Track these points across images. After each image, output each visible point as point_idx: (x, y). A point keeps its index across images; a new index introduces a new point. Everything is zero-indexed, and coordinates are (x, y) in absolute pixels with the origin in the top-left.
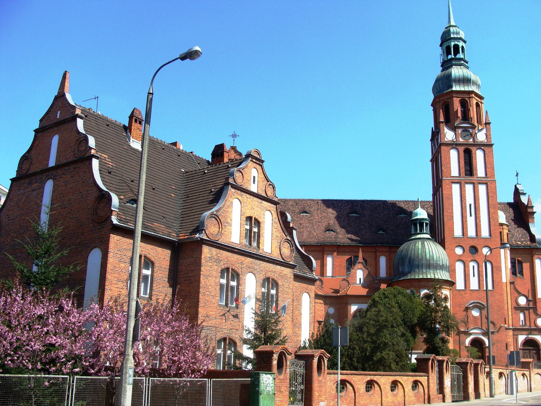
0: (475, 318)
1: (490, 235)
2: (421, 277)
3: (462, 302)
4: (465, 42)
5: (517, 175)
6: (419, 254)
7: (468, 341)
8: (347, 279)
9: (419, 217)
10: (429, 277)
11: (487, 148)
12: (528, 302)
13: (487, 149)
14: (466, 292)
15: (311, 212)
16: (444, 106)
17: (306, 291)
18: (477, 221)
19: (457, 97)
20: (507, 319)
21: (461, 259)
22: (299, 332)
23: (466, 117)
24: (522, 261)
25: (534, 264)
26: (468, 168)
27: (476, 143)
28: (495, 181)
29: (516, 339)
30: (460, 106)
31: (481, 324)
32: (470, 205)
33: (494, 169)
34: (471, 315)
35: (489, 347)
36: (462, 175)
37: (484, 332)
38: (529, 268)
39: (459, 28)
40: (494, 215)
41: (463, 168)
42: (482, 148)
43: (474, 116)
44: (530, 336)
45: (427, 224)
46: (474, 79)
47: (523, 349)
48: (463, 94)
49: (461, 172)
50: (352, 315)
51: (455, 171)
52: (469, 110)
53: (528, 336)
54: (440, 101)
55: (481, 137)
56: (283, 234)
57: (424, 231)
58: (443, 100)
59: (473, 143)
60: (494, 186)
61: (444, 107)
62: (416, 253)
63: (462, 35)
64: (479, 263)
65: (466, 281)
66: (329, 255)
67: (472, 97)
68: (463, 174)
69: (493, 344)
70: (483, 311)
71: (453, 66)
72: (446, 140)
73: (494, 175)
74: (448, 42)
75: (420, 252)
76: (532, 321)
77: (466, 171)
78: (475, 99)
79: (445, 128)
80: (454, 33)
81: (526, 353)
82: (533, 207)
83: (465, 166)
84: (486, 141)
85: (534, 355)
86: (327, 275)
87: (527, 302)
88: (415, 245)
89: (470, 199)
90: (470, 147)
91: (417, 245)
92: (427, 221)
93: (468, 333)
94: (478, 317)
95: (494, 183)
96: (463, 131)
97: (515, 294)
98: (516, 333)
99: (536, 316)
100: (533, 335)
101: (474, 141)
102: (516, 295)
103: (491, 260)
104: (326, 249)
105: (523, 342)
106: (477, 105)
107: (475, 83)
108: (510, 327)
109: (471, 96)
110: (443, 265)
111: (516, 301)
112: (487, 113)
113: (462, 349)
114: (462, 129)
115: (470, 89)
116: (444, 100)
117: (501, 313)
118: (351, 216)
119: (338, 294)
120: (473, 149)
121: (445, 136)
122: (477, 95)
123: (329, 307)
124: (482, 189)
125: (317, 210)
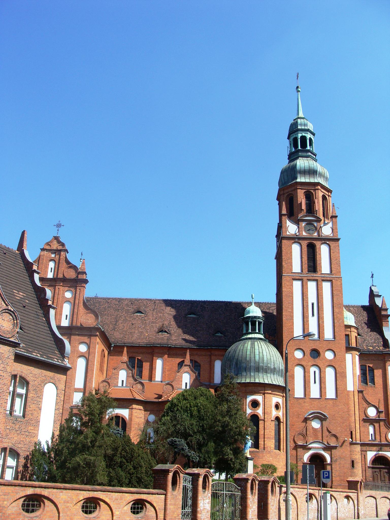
0: (315, 430)
1: (334, 337)
2: (248, 381)
3: (301, 412)
4: (314, 134)
5: (372, 277)
6: (247, 357)
7: (306, 457)
8: (172, 384)
9: (251, 315)
10: (257, 381)
11: (333, 242)
12: (378, 414)
13: (333, 244)
14: (306, 401)
15: (146, 311)
16: (288, 198)
17: (52, 381)
18: (320, 322)
19: (301, 189)
20: (354, 433)
22: (36, 432)
23: (311, 210)
24: (374, 368)
25: (387, 372)
26: (312, 264)
27: (321, 237)
28: (340, 278)
29: (364, 455)
30: (305, 199)
31: (322, 437)
32: (313, 304)
33: (340, 266)
34: (311, 427)
35: (331, 465)
36: (304, 272)
37: (324, 446)
38: (381, 375)
39: (307, 120)
40: (338, 315)
41: (305, 264)
42: (328, 242)
43: (319, 209)
44: (380, 452)
45: (260, 323)
46: (321, 171)
47: (372, 468)
48: (307, 186)
49: (303, 268)
51: (296, 267)
52: (314, 203)
53: (378, 452)
54: (284, 194)
55: (327, 231)
56: (3, 303)
57: (255, 330)
58: (287, 193)
59: (317, 237)
60: (339, 283)
61: (288, 200)
62: (244, 353)
63: (310, 126)
64: (321, 368)
66: (159, 357)
67: (318, 189)
68: (306, 270)
69: (336, 461)
70: (324, 422)
71: (300, 158)
72: (288, 233)
73: (340, 272)
74: (296, 133)
75: (248, 353)
76: (383, 436)
77: (309, 266)
78: (322, 191)
79: (288, 221)
80: (301, 125)
81: (375, 472)
82: (387, 310)
83: (308, 262)
84: (332, 235)
85: (385, 474)
86: (156, 380)
87: (377, 414)
88: (244, 345)
89: (312, 298)
90: (313, 242)
91: (246, 345)
92: (261, 319)
93: (307, 447)
95: (340, 280)
96: (307, 224)
97: (363, 405)
98: (364, 448)
99: (387, 430)
100: (384, 451)
101: (319, 235)
102: (365, 406)
103: (334, 366)
104: (156, 351)
105: (373, 459)
106: (324, 198)
107: (321, 175)
108: (357, 442)
109: (317, 188)
110: (275, 368)
111: (365, 412)
112: (333, 206)
114: (306, 222)
115: (316, 181)
116: (288, 192)
118: (188, 317)
119: (160, 400)
120: (317, 243)
121: (287, 229)
122: (323, 187)
123: (150, 414)
124: (326, 286)
125: (153, 310)
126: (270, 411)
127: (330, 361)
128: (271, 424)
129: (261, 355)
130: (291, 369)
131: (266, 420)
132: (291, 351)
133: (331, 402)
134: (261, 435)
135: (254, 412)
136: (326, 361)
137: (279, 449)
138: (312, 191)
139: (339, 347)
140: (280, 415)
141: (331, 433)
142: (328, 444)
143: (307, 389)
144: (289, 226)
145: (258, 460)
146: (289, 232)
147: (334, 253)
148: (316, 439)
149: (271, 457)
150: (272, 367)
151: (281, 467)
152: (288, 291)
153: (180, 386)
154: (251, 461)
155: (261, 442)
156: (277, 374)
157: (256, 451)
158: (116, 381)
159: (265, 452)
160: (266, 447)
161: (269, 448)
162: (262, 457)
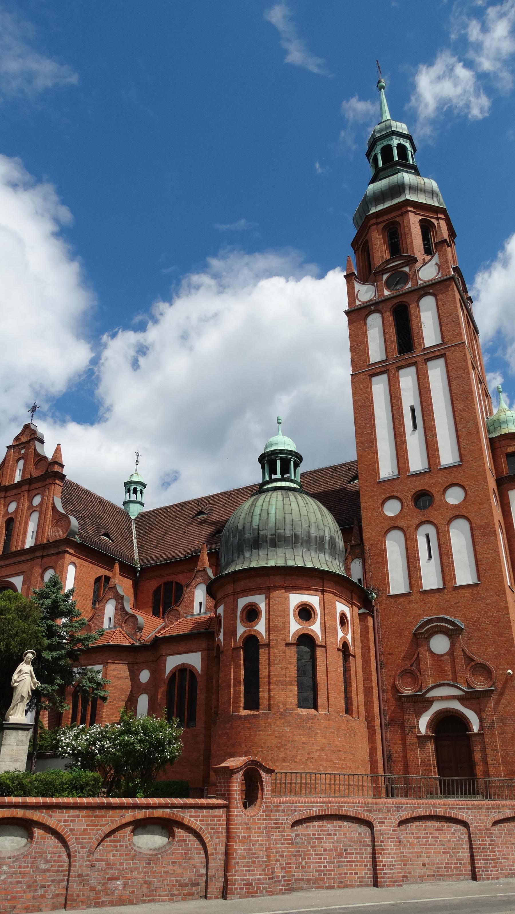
3: (405, 623)
14: (412, 598)
19: (377, 224)
21: (396, 525)
35: (481, 735)
37: (462, 693)
42: (431, 291)
50: (167, 681)
64: (439, 525)
65: (412, 572)
69: (492, 726)
72: (358, 303)
75: (243, 516)
78: (416, 214)
92: (286, 454)
94: (446, 657)
103: (466, 515)
113: (412, 744)
117: (505, 639)
122: (419, 206)
125: (223, 506)
126: (284, 623)
127: (456, 507)
128: (284, 653)
129: (264, 515)
130: (379, 540)
131: (272, 643)
132: (376, 505)
133: (466, 593)
134: (264, 678)
135: (250, 631)
136: (447, 509)
137: (316, 707)
138: (397, 219)
139: (471, 475)
140: (312, 631)
141: (473, 660)
142: (469, 686)
143: (413, 574)
144: (359, 291)
145: (256, 735)
146: (360, 301)
147: (444, 305)
148: (443, 680)
149: (287, 727)
150: (288, 533)
151: (319, 748)
152: (362, 399)
154: (20, 732)
155: (263, 694)
156: (304, 544)
157: (253, 715)
158: (100, 621)
159: (270, 716)
160: (274, 704)
161: (281, 706)
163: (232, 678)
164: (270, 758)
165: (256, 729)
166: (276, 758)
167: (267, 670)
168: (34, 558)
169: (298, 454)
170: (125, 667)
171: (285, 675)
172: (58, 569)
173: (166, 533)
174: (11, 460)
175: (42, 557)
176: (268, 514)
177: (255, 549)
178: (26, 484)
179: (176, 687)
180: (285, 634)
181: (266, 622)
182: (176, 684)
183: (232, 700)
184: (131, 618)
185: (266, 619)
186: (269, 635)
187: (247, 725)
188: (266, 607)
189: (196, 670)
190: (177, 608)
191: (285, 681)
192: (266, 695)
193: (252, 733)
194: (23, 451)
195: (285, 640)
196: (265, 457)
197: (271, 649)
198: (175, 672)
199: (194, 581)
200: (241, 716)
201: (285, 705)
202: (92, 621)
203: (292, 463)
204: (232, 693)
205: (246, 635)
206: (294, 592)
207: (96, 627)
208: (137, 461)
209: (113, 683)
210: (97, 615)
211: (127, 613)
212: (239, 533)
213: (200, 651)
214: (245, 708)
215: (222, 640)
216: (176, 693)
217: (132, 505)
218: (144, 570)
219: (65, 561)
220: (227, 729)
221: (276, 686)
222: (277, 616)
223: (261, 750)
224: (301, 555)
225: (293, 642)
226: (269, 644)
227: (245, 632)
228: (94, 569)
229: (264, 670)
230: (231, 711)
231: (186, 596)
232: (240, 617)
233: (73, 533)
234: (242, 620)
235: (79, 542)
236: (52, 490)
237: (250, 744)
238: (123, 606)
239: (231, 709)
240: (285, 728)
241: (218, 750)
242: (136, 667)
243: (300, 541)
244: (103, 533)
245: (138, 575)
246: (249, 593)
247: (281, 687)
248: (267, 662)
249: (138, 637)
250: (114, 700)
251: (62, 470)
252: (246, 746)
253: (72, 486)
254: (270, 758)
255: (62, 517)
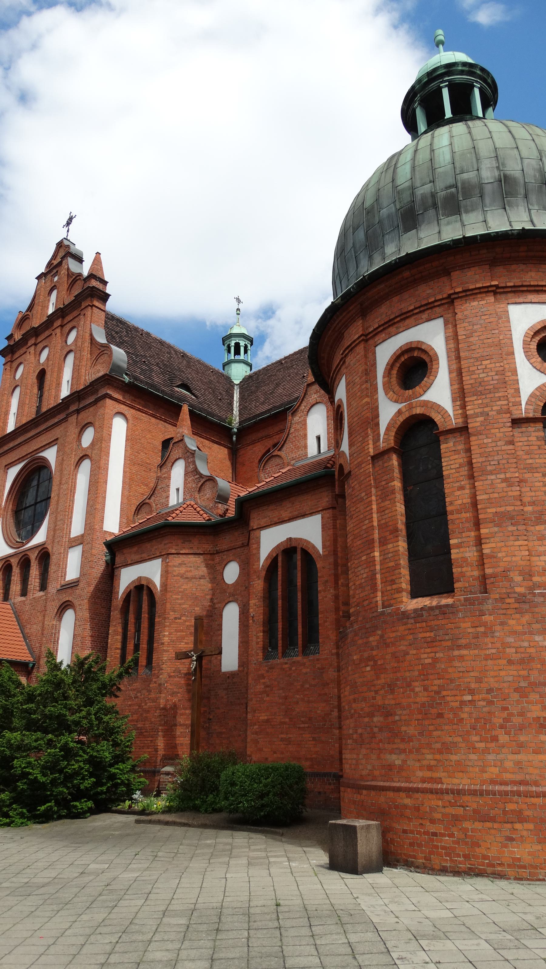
50: (263, 573)
92: (462, 72)
126: (502, 373)
128: (512, 443)
131: (474, 424)
134: (459, 512)
135: (410, 407)
145: (451, 659)
153: (301, 452)
156: (533, 198)
157: (439, 607)
158: (164, 495)
159: (488, 606)
160: (494, 576)
161: (518, 579)
162: (476, 637)
163: (375, 524)
164: (498, 721)
165: (449, 643)
166: (517, 720)
167: (467, 491)
168: (67, 415)
169: (488, 74)
170: (198, 560)
171: (520, 498)
172: (97, 424)
173: (278, 385)
174: (42, 294)
175: (78, 411)
176: (432, 151)
177: (407, 230)
178: (58, 319)
179: (280, 583)
180: (506, 398)
181: (451, 380)
182: (280, 578)
183: (378, 576)
184: (208, 483)
185: (450, 372)
186: (463, 407)
187: (421, 635)
188: (447, 344)
189: (314, 547)
190: (279, 453)
191: (522, 513)
192: (471, 554)
193: (439, 655)
194: (56, 279)
195: (509, 412)
196: (415, 95)
197: (472, 438)
198: (277, 555)
199: (304, 404)
200: (404, 613)
201: (528, 574)
202: (153, 498)
203: (477, 92)
204: (378, 559)
205: (401, 419)
206: (521, 300)
207: (159, 506)
208: (238, 310)
209: (179, 587)
210: (159, 487)
211: (201, 476)
212: (368, 213)
213: (317, 512)
214: (414, 595)
215: (347, 452)
216: (280, 593)
217: (234, 366)
218: (243, 431)
219: (107, 411)
220: (372, 649)
221: (496, 529)
222: (482, 358)
223: (469, 698)
224: (529, 219)
225: (531, 415)
226: (467, 427)
227: (399, 412)
228: (160, 426)
229: (458, 493)
230: (380, 603)
231: (292, 430)
232: (384, 384)
233: (116, 368)
234: (387, 388)
235: (127, 382)
236: (89, 316)
237: (436, 682)
238: (196, 466)
239: (379, 598)
240: (537, 638)
241: (355, 701)
242: (217, 558)
243: (522, 191)
244: (179, 383)
245: (234, 439)
246: (401, 324)
247: (511, 528)
248: (464, 471)
249: (221, 512)
250: (182, 615)
251: (105, 289)
252: (426, 689)
253: (138, 332)
254: (498, 721)
255: (103, 349)
